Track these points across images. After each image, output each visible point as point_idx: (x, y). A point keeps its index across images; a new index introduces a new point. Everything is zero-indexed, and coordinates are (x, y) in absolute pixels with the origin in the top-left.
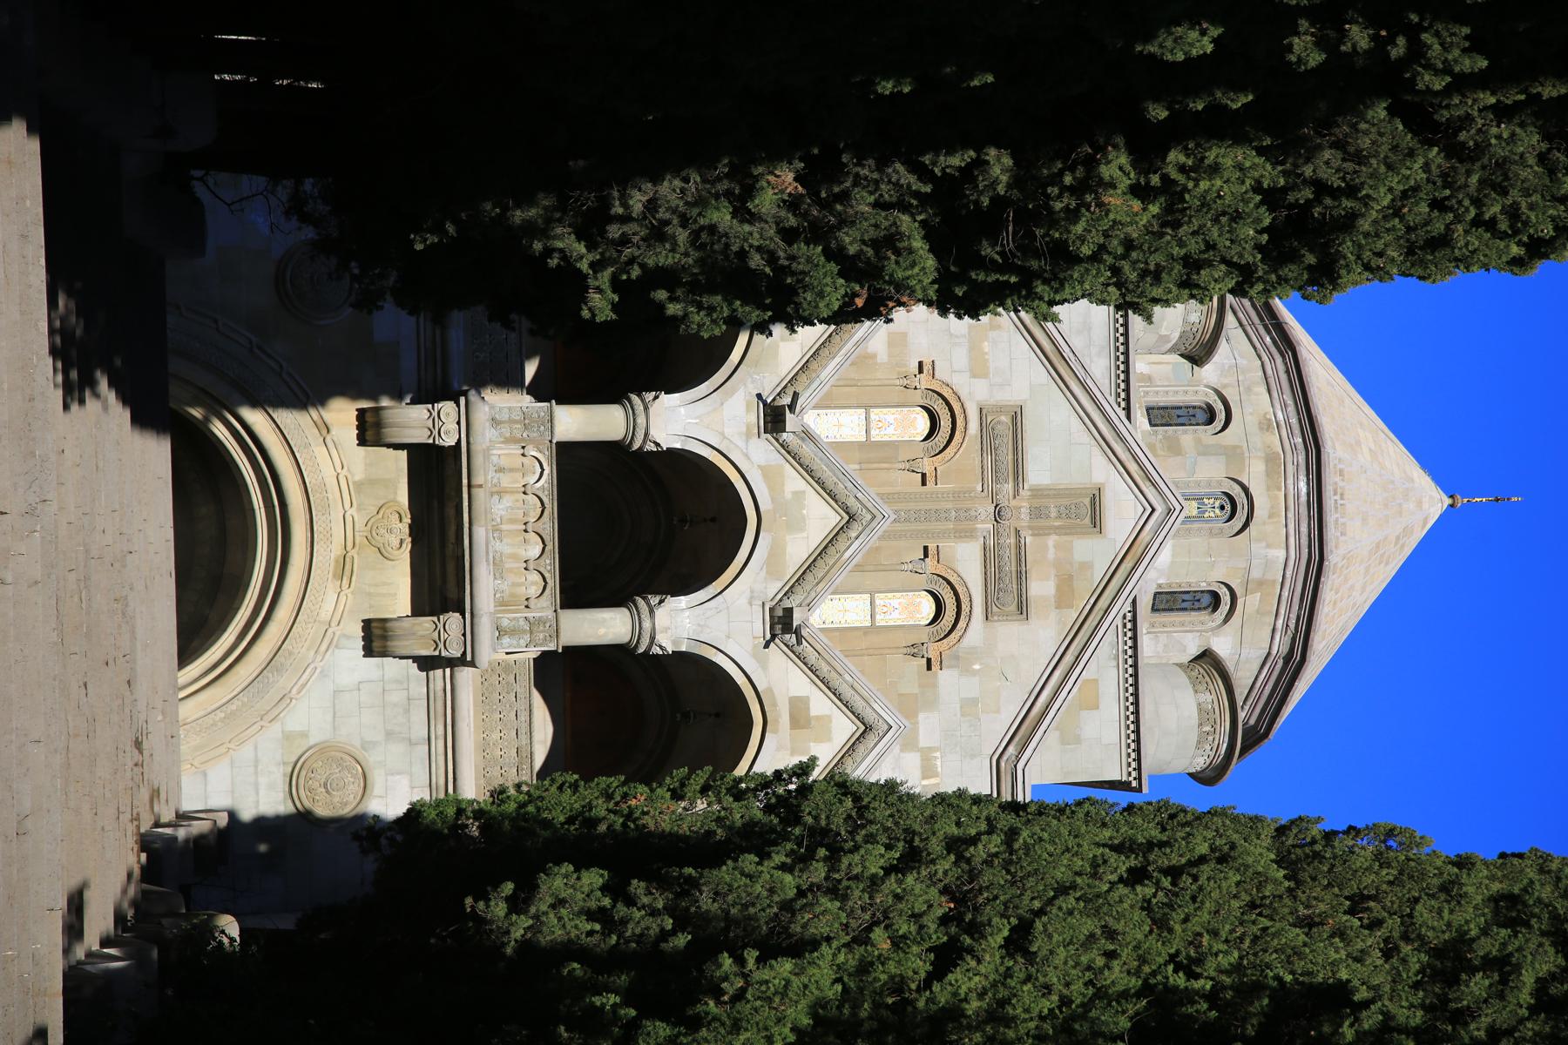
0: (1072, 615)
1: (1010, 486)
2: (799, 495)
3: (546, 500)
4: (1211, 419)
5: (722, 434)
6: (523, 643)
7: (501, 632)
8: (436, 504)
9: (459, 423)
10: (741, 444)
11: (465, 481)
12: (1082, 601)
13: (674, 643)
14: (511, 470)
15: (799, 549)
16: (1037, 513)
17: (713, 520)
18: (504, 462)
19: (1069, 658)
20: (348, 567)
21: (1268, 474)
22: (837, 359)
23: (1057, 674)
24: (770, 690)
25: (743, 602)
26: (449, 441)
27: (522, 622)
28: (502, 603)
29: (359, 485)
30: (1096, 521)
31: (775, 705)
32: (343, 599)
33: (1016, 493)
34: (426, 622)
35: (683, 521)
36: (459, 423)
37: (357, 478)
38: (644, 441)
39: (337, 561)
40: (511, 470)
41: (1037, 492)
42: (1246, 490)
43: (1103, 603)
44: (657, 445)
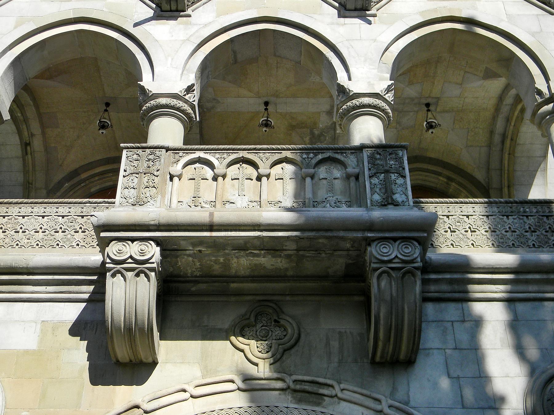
3: (233, 156)
5: (184, 41)
6: (400, 181)
7: (388, 201)
8: (233, 285)
10: (195, 28)
13: (382, 79)
14: (197, 189)
17: (266, 104)
18: (187, 198)
20: (307, 387)
24: (422, 13)
25: (341, 30)
26: (153, 252)
27: (375, 181)
28: (358, 200)
29: (206, 371)
31: (435, 10)
32: (347, 395)
34: (380, 287)
35: (267, 124)
37: (199, 374)
38: (186, 101)
39: (299, 401)
40: (197, 189)
44: (189, 89)
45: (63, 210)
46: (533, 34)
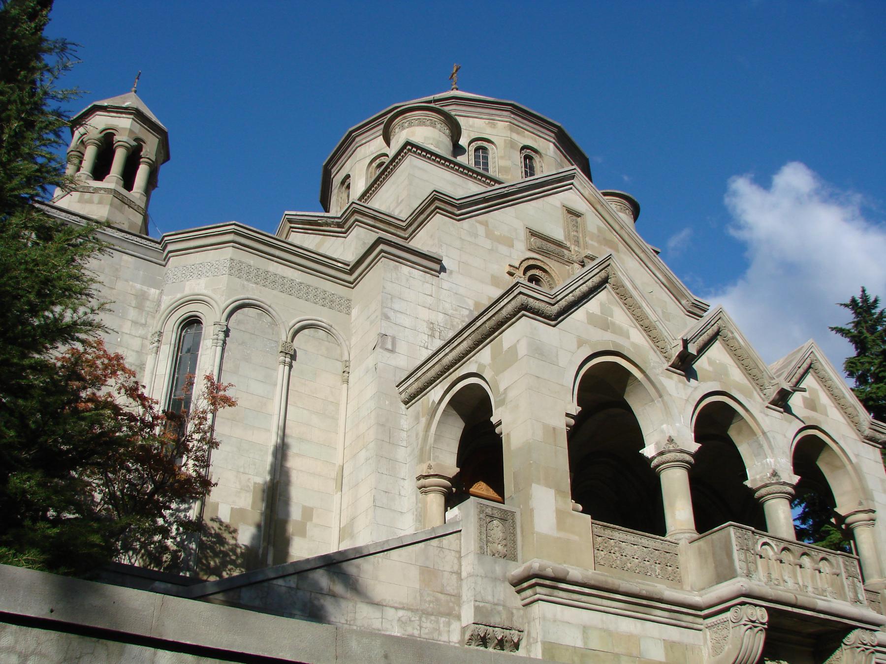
0: (621, 246)
1: (566, 252)
2: (711, 362)
4: (484, 149)
9: (756, 605)
11: (789, 609)
12: (615, 238)
15: (736, 375)
16: (577, 243)
19: (642, 255)
21: (518, 133)
22: (644, 305)
23: (650, 265)
30: (578, 215)
33: (568, 249)
36: (756, 605)
41: (568, 237)
42: (524, 148)
43: (617, 227)
45: (645, 541)
46: (857, 456)
